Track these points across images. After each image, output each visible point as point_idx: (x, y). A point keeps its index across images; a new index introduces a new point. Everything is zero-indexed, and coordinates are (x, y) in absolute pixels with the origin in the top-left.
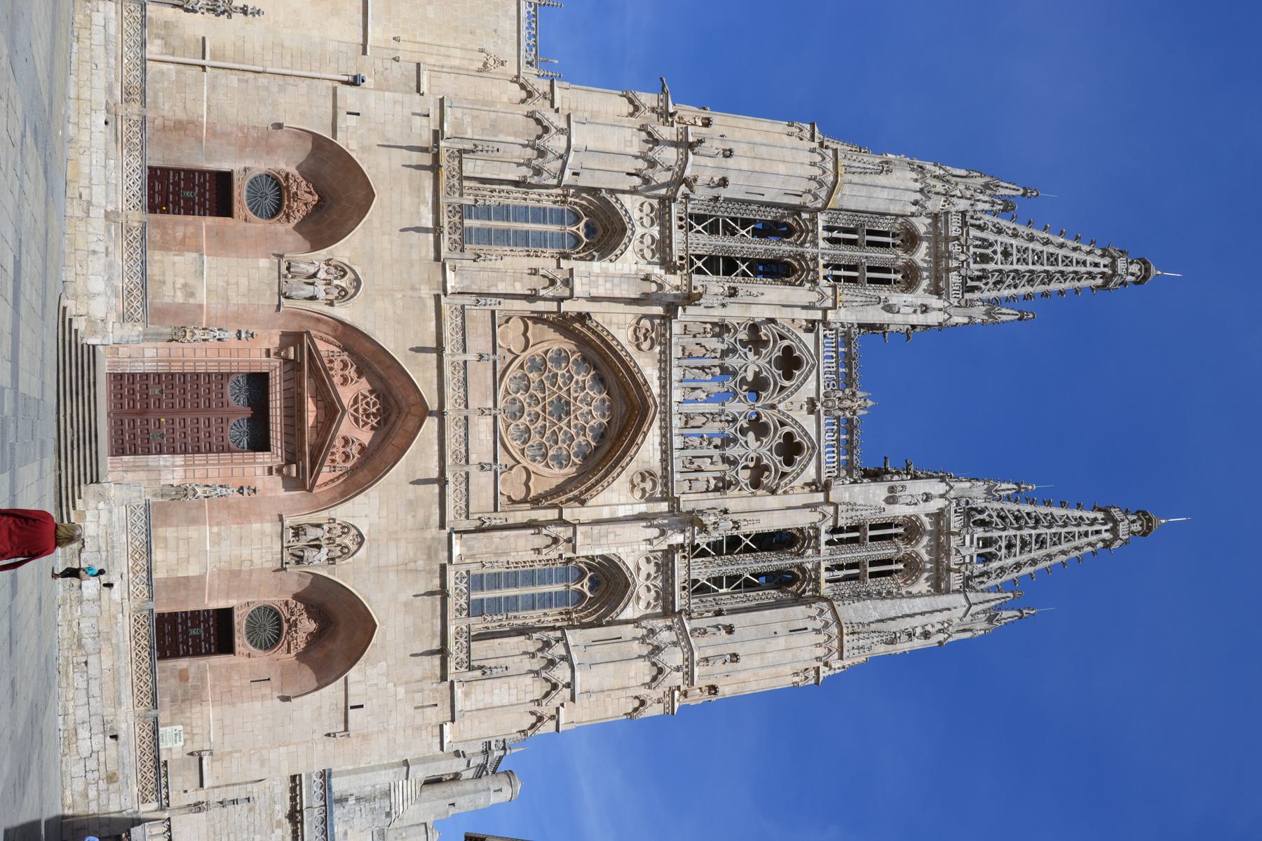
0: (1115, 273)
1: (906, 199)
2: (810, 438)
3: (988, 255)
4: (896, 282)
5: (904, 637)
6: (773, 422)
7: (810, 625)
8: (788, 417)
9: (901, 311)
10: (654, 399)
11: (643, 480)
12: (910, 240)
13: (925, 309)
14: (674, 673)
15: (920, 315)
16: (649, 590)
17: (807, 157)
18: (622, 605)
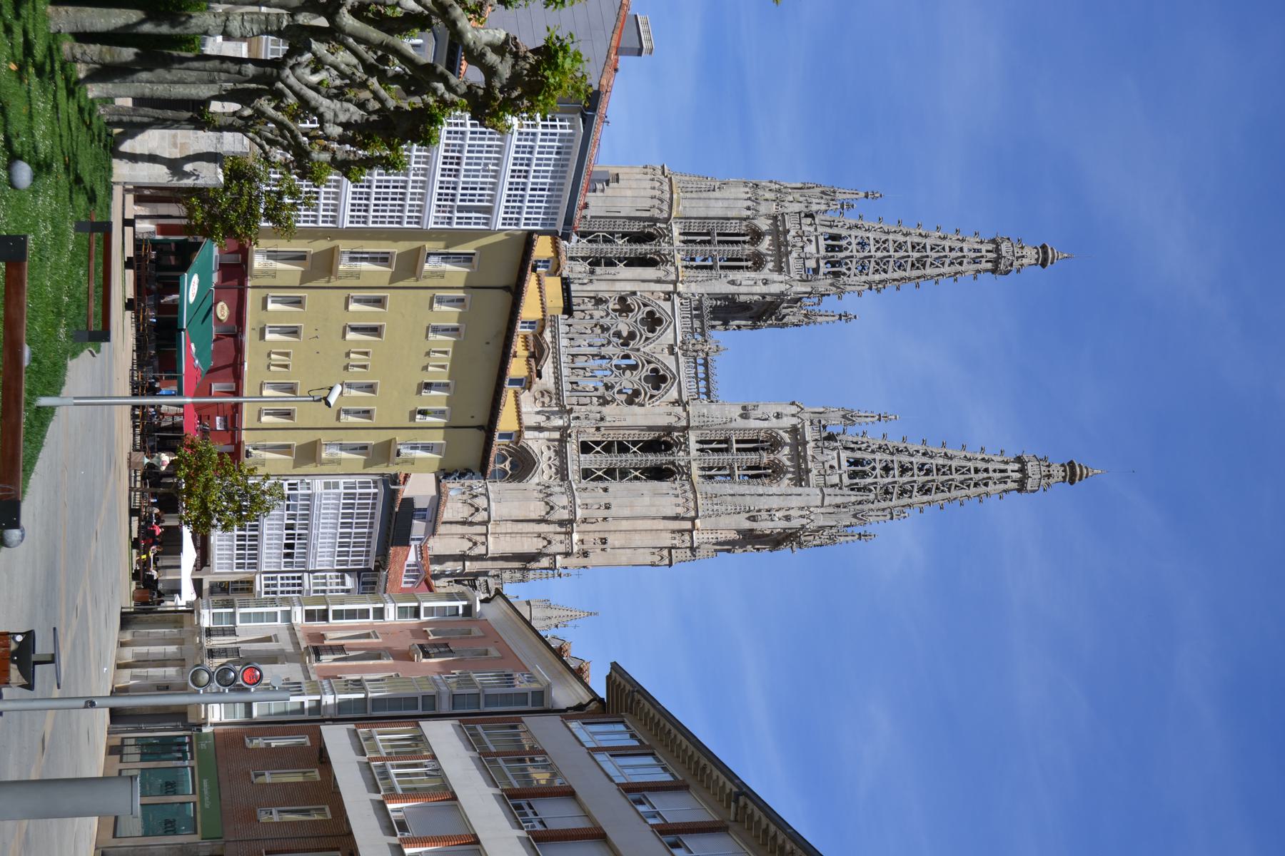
0: (1000, 257)
1: (740, 206)
2: (671, 371)
3: (842, 246)
4: (747, 267)
5: (764, 515)
6: (641, 361)
7: (672, 492)
8: (652, 356)
9: (743, 283)
10: (547, 344)
11: (543, 395)
12: (757, 236)
13: (766, 282)
14: (562, 510)
15: (764, 287)
16: (551, 468)
17: (648, 184)
18: (530, 475)
